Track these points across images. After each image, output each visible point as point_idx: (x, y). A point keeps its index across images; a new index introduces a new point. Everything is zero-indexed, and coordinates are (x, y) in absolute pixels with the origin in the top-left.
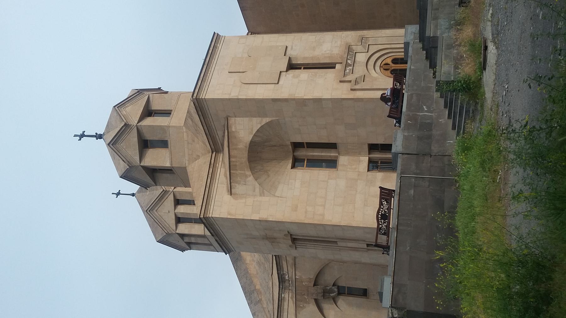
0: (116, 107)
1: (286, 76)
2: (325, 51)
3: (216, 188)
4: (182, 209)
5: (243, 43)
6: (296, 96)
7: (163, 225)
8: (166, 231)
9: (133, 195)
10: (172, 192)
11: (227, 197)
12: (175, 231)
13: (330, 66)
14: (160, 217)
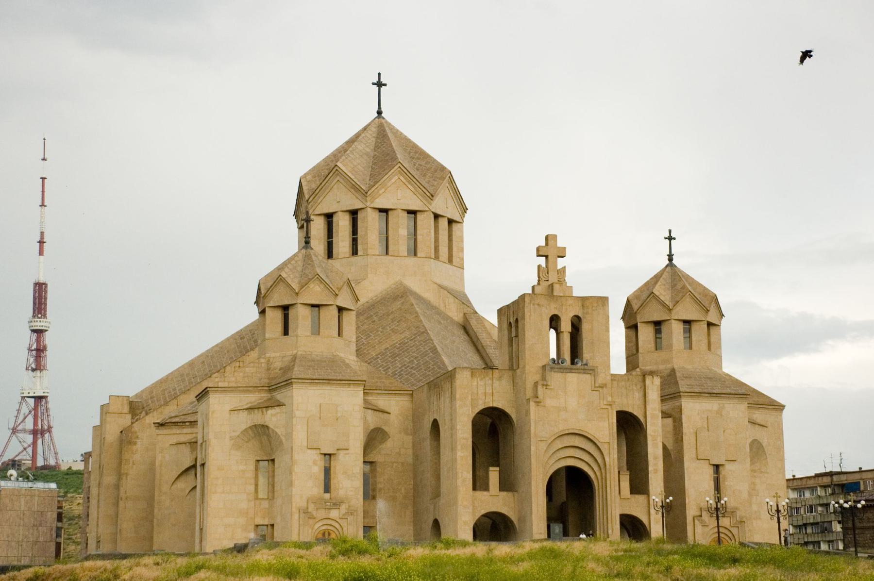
0: (317, 276)
1: (316, 454)
2: (341, 483)
3: (236, 396)
4: (343, 223)
5: (354, 409)
6: (296, 466)
7: (320, 193)
8: (311, 199)
9: (379, 113)
10: (364, 206)
11: (228, 407)
12: (313, 214)
13: (327, 489)
14: (330, 188)
